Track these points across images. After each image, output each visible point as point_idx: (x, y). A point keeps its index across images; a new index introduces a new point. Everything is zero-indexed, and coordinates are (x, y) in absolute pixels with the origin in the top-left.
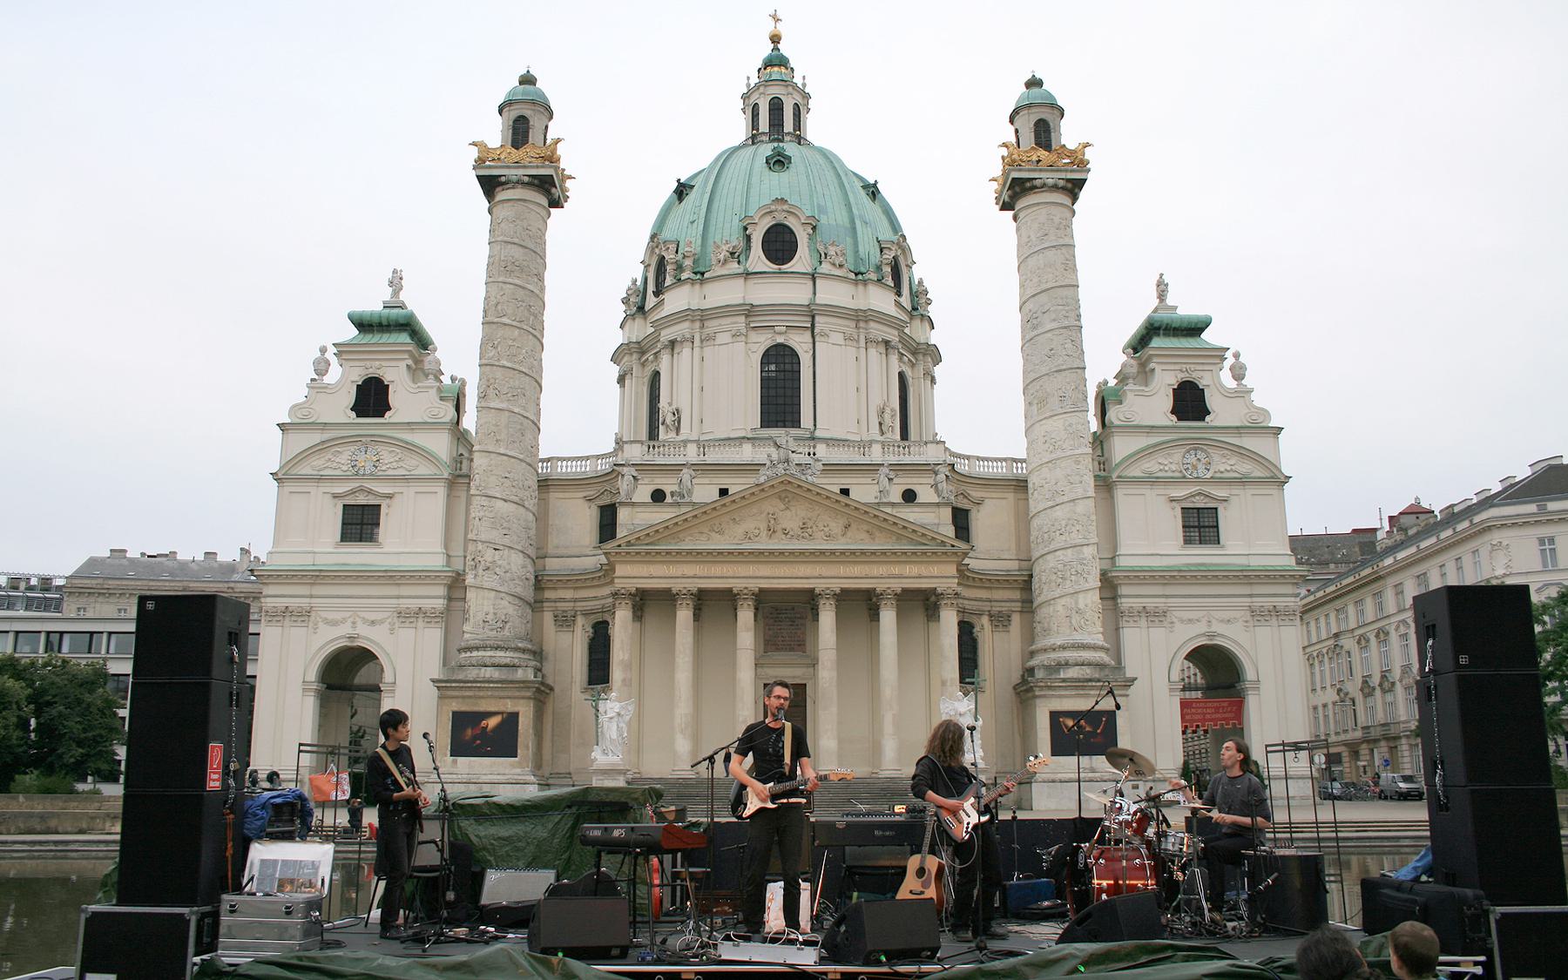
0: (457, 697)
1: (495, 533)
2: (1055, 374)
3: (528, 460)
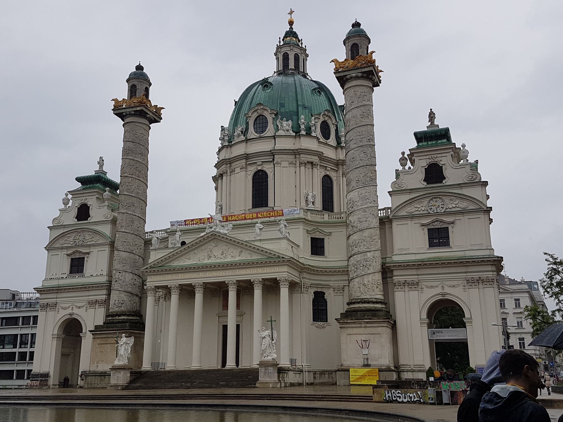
0: (100, 338)
1: (119, 265)
2: (355, 170)
3: (135, 233)
